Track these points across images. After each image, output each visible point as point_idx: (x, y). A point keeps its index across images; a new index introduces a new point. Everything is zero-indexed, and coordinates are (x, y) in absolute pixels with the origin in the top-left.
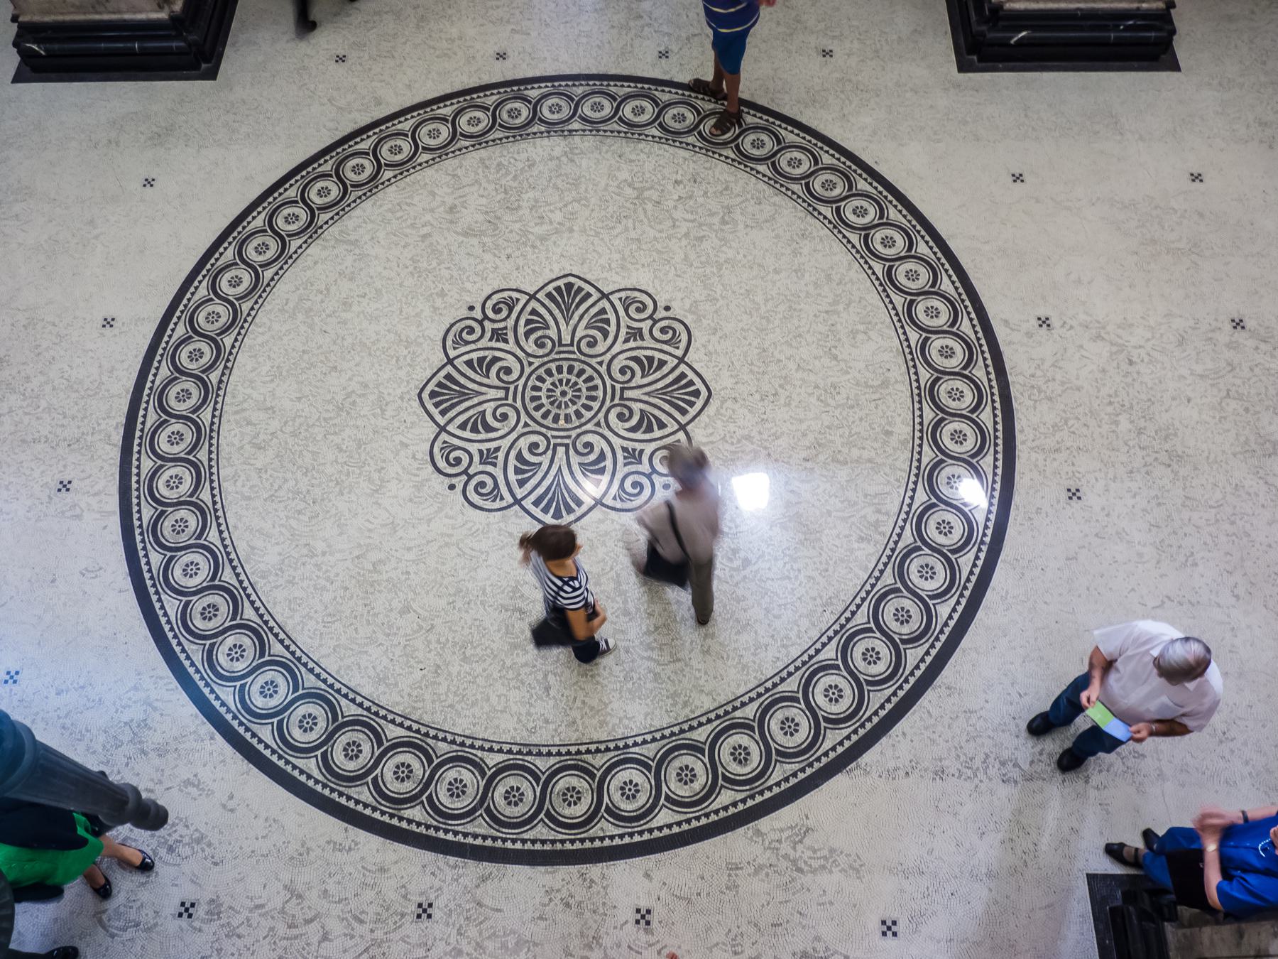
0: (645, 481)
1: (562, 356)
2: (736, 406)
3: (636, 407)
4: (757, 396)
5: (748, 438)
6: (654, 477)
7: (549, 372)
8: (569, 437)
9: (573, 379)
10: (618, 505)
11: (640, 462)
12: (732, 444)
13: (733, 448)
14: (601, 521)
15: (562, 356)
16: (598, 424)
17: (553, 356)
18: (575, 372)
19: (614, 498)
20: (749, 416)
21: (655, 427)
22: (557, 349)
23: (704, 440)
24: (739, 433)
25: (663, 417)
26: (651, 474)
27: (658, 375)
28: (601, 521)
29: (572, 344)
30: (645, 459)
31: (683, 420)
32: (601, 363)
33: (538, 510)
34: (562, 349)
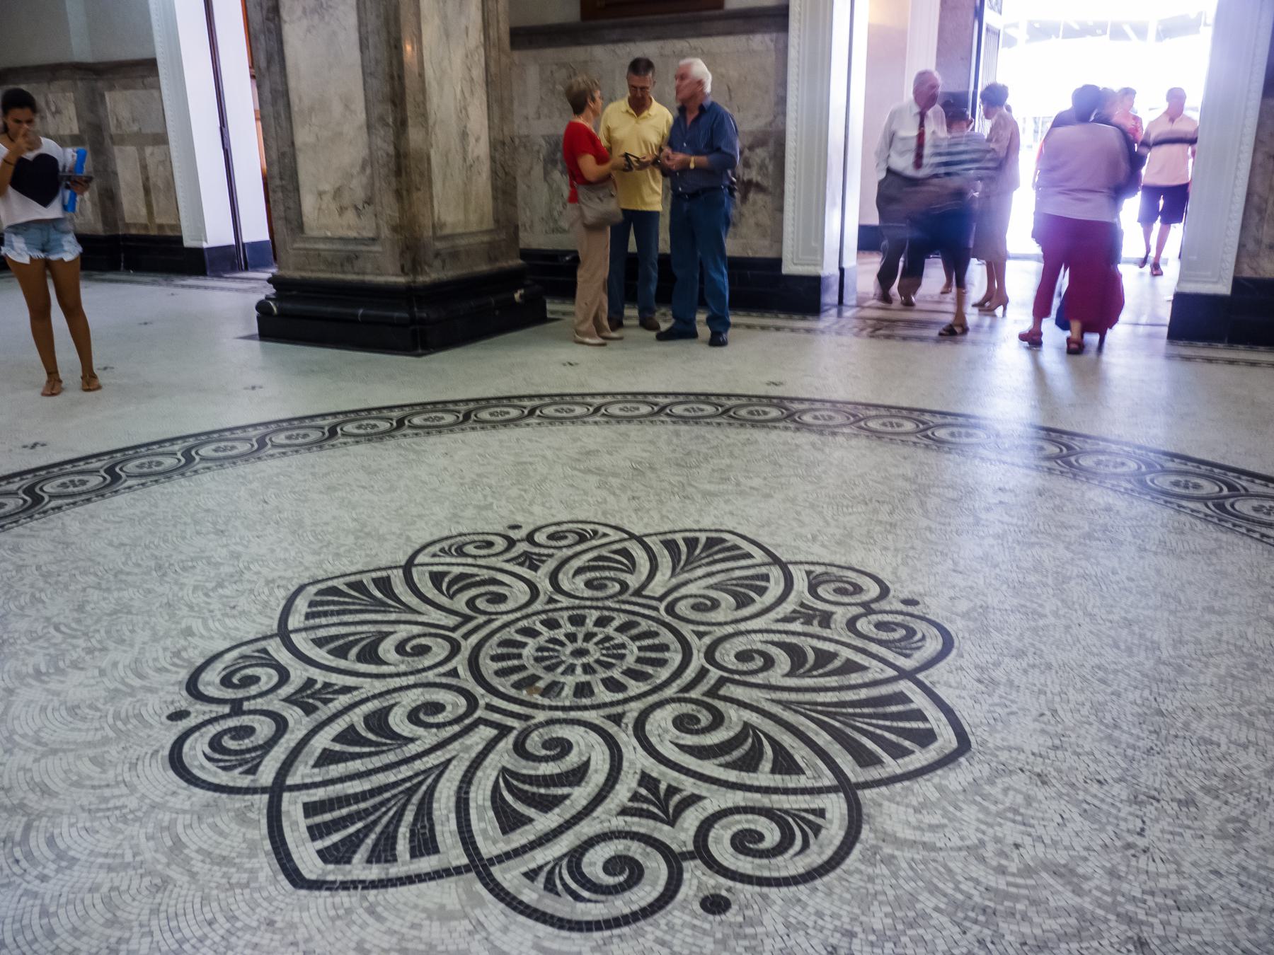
0: (657, 869)
1: (627, 607)
2: (1040, 793)
3: (736, 716)
4: (1121, 791)
5: (1065, 873)
6: (688, 865)
7: (578, 621)
8: (527, 718)
9: (620, 638)
10: (530, 895)
11: (672, 822)
12: (1002, 871)
13: (1001, 883)
14: (443, 915)
15: (627, 607)
16: (617, 719)
17: (609, 603)
18: (634, 632)
19: (531, 875)
20: (1078, 822)
21: (766, 765)
22: (625, 597)
23: (909, 834)
24: (1032, 852)
25: (800, 753)
26: (690, 856)
27: (833, 681)
28: (443, 915)
29: (661, 599)
30: (691, 819)
31: (853, 772)
32: (700, 635)
33: (303, 823)
34: (634, 599)
